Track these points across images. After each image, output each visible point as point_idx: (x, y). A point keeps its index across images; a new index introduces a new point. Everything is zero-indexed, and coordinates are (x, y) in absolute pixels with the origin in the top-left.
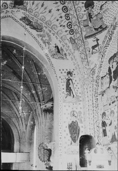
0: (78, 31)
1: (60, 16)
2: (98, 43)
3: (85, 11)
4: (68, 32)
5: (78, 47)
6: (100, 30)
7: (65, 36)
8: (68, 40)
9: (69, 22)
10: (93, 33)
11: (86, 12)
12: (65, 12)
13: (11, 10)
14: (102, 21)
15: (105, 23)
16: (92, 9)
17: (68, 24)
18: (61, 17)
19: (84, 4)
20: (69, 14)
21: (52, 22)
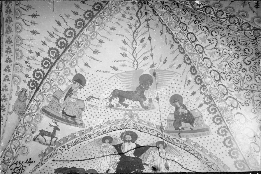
0: (45, 93)
1: (38, 51)
2: (54, 132)
3: (70, 81)
4: (28, 79)
5: (27, 112)
6: (69, 119)
7: (20, 80)
8: (18, 88)
9: (41, 70)
10: (57, 115)
11: (70, 84)
14: (81, 113)
15: (83, 118)
16: (79, 88)
17: (38, 72)
18: (38, 54)
19: (76, 74)
21: (22, 45)
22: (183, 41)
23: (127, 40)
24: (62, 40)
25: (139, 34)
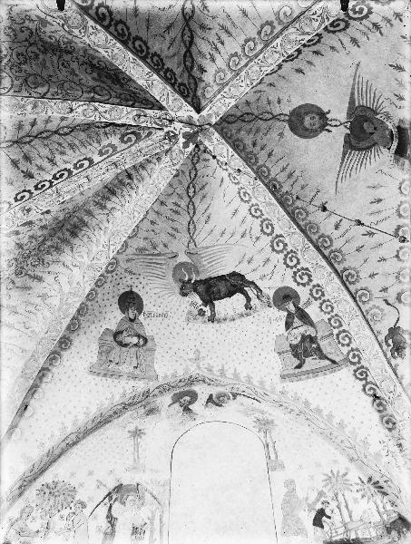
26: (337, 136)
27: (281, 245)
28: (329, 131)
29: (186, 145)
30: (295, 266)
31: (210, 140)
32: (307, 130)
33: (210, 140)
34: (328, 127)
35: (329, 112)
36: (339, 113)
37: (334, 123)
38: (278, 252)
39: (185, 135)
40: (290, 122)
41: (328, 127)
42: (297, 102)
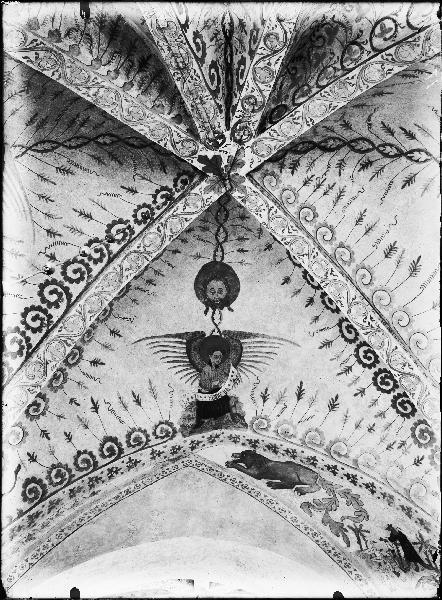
9: (416, 425)
12: (389, 392)
13: (189, 439)
17: (417, 433)
20: (405, 395)
22: (387, 67)
23: (407, 174)
24: (361, 354)
25: (390, 139)
26: (199, 320)
27: (54, 298)
28: (206, 312)
29: (202, 159)
30: (28, 327)
31: (207, 190)
32: (206, 283)
33: (207, 190)
34: (211, 310)
35: (230, 309)
36: (230, 321)
37: (217, 316)
38: (41, 294)
39: (217, 159)
40: (214, 262)
41: (211, 310)
42: (239, 271)
